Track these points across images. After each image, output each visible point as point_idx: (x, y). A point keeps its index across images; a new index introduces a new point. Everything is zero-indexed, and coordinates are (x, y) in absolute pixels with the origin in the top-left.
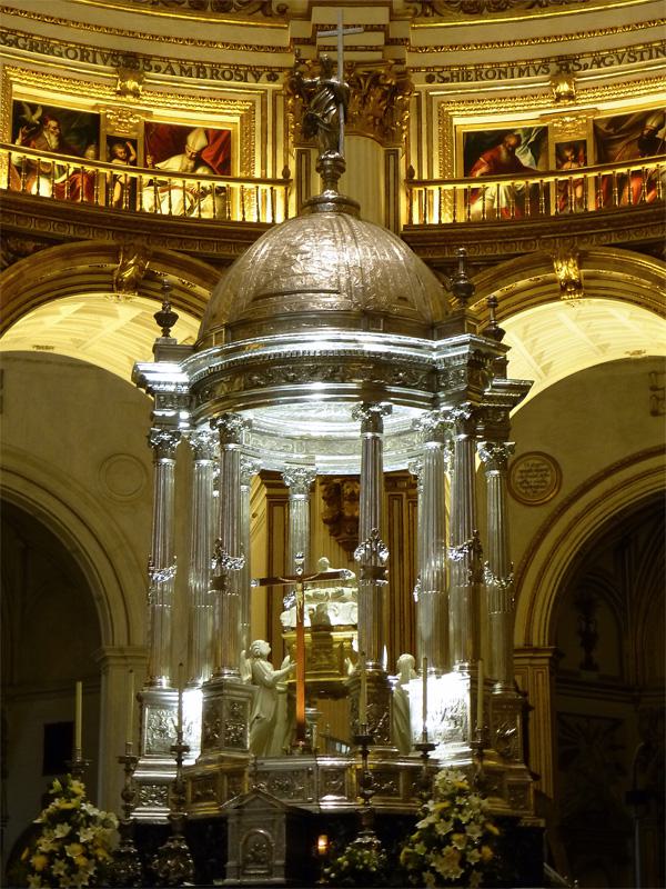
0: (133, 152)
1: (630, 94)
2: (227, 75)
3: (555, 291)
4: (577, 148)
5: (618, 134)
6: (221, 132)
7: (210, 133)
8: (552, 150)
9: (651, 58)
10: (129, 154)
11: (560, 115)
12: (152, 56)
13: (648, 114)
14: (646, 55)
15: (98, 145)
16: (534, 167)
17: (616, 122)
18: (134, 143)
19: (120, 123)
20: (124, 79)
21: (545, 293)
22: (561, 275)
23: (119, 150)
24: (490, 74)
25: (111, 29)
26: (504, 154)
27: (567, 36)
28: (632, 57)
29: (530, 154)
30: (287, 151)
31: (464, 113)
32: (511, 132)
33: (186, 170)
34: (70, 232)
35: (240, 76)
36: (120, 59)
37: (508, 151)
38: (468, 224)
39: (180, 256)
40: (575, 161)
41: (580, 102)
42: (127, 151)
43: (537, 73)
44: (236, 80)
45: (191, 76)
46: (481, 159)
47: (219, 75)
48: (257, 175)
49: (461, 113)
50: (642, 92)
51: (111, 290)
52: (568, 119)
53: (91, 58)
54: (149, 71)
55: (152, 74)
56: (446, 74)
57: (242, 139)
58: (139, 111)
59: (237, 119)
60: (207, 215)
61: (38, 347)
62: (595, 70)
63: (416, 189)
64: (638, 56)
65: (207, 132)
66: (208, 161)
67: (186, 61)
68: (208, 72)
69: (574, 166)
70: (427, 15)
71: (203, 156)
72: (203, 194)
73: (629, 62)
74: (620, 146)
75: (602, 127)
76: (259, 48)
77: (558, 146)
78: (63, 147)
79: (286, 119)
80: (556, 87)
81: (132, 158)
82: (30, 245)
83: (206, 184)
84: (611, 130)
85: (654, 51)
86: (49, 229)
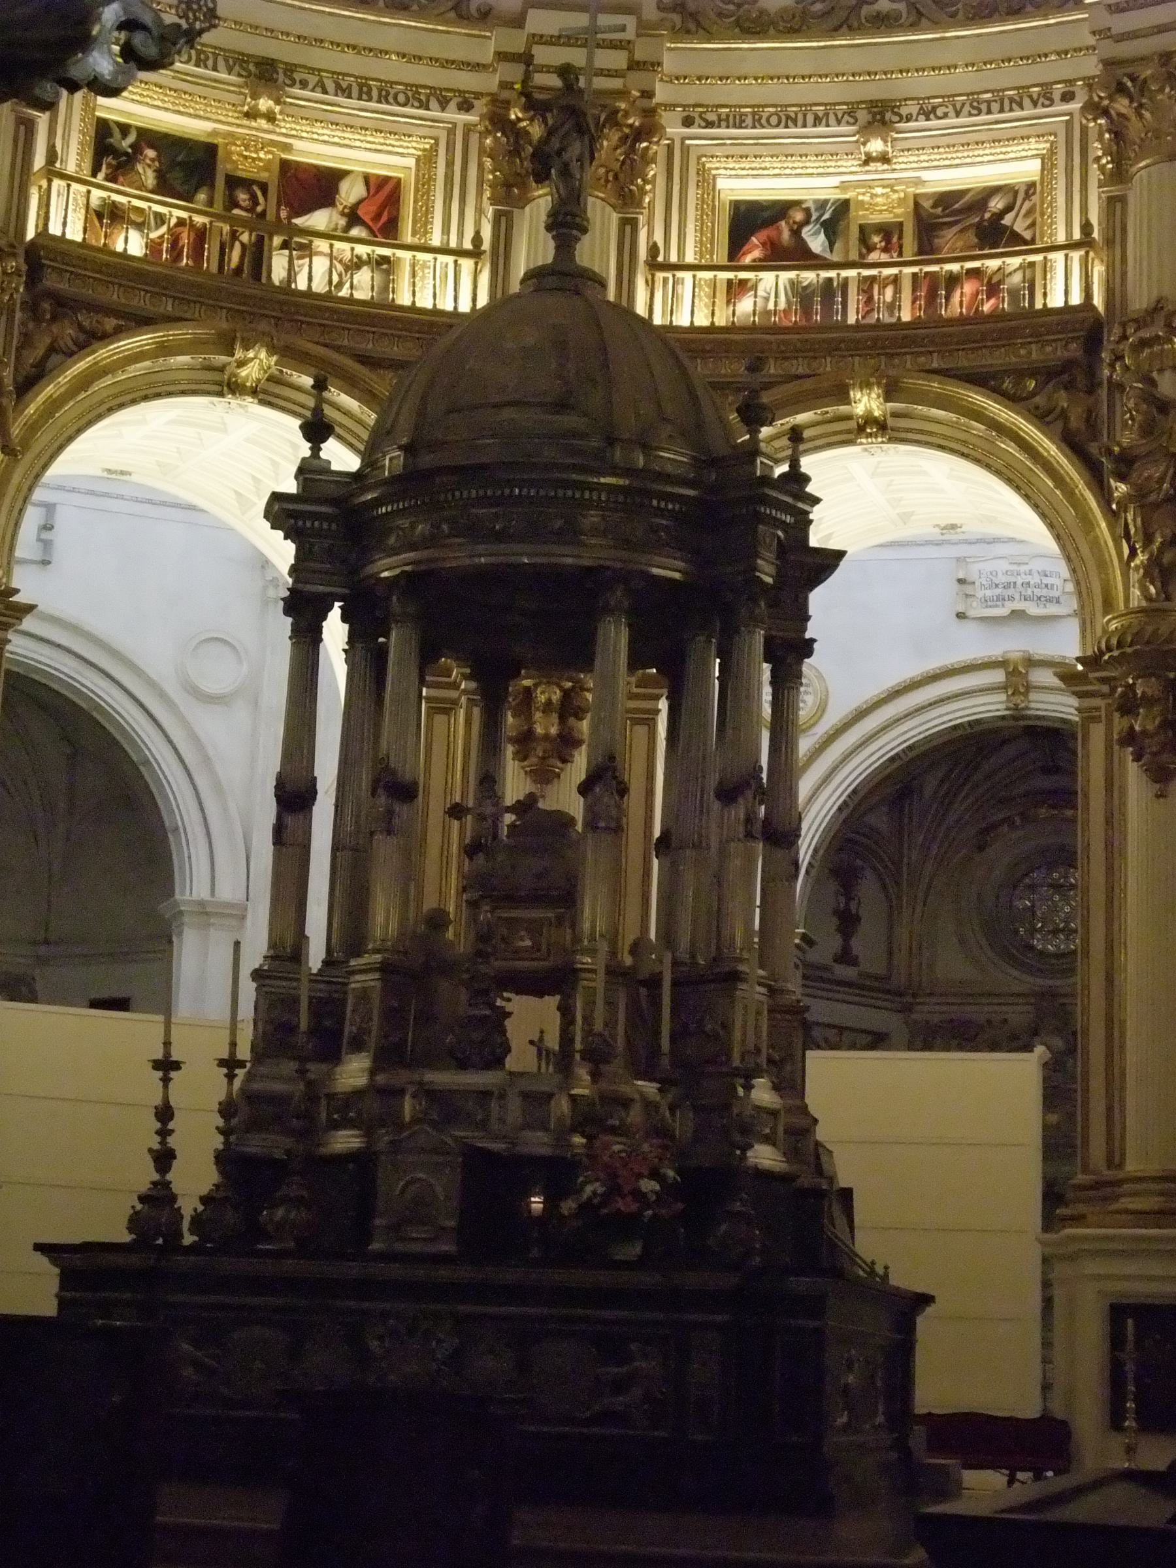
0: (261, 199)
1: (968, 160)
2: (401, 98)
3: (849, 432)
4: (889, 232)
5: (947, 216)
6: (387, 179)
7: (372, 181)
8: (854, 232)
9: (1002, 111)
10: (255, 202)
11: (867, 185)
12: (296, 65)
14: (995, 106)
15: (212, 186)
16: (828, 255)
17: (946, 199)
18: (264, 187)
19: (246, 157)
20: (255, 96)
21: (840, 432)
22: (859, 409)
23: (242, 197)
24: (774, 120)
25: (241, 24)
26: (786, 235)
27: (885, 73)
28: (974, 108)
29: (822, 237)
30: (480, 211)
31: (733, 172)
32: (797, 203)
33: (335, 229)
34: (169, 307)
35: (420, 101)
36: (252, 67)
37: (791, 230)
38: (731, 329)
39: (322, 351)
40: (886, 250)
41: (897, 167)
42: (253, 198)
43: (839, 122)
44: (413, 106)
45: (350, 97)
46: (754, 239)
47: (391, 99)
48: (436, 240)
49: (729, 172)
50: (986, 159)
51: (221, 394)
52: (879, 191)
53: (210, 63)
54: (291, 86)
55: (296, 91)
56: (712, 117)
57: (417, 190)
58: (273, 143)
59: (411, 162)
60: (362, 295)
61: (109, 471)
62: (923, 123)
63: (660, 275)
64: (984, 107)
65: (367, 178)
66: (367, 219)
67: (345, 75)
68: (375, 93)
69: (884, 257)
70: (688, 32)
71: (360, 212)
72: (356, 264)
73: (970, 115)
74: (950, 233)
75: (927, 204)
76: (447, 64)
77: (862, 228)
78: (164, 187)
79: (481, 165)
80: (864, 144)
81: (259, 209)
82: (110, 323)
83: (362, 250)
85: (1007, 102)
86: (140, 302)
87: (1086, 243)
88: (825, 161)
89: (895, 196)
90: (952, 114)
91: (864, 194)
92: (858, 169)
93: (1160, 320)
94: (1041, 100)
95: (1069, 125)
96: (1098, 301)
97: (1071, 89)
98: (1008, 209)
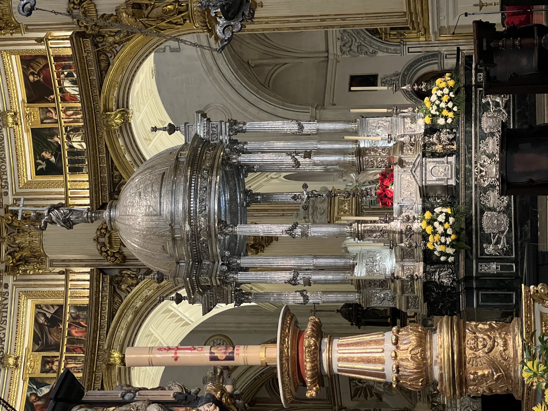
4: (45, 361)
8: (44, 375)
9: (6, 312)
13: (36, 321)
17: (36, 339)
21: (125, 375)
22: (118, 361)
26: (39, 403)
28: (3, 323)
32: (27, 398)
37: (38, 400)
40: (53, 363)
41: (21, 355)
52: (28, 364)
62: (5, 343)
69: (56, 363)
73: (6, 324)
75: (37, 347)
77: (42, 372)
80: (10, 365)
84: (40, 343)
87: (66, 273)
88: (13, 382)
89: (32, 359)
90: (4, 331)
91: (29, 370)
92: (19, 370)
93: (101, 240)
94: (5, 296)
95: (17, 286)
96: (88, 269)
97: (3, 285)
98: (44, 315)
